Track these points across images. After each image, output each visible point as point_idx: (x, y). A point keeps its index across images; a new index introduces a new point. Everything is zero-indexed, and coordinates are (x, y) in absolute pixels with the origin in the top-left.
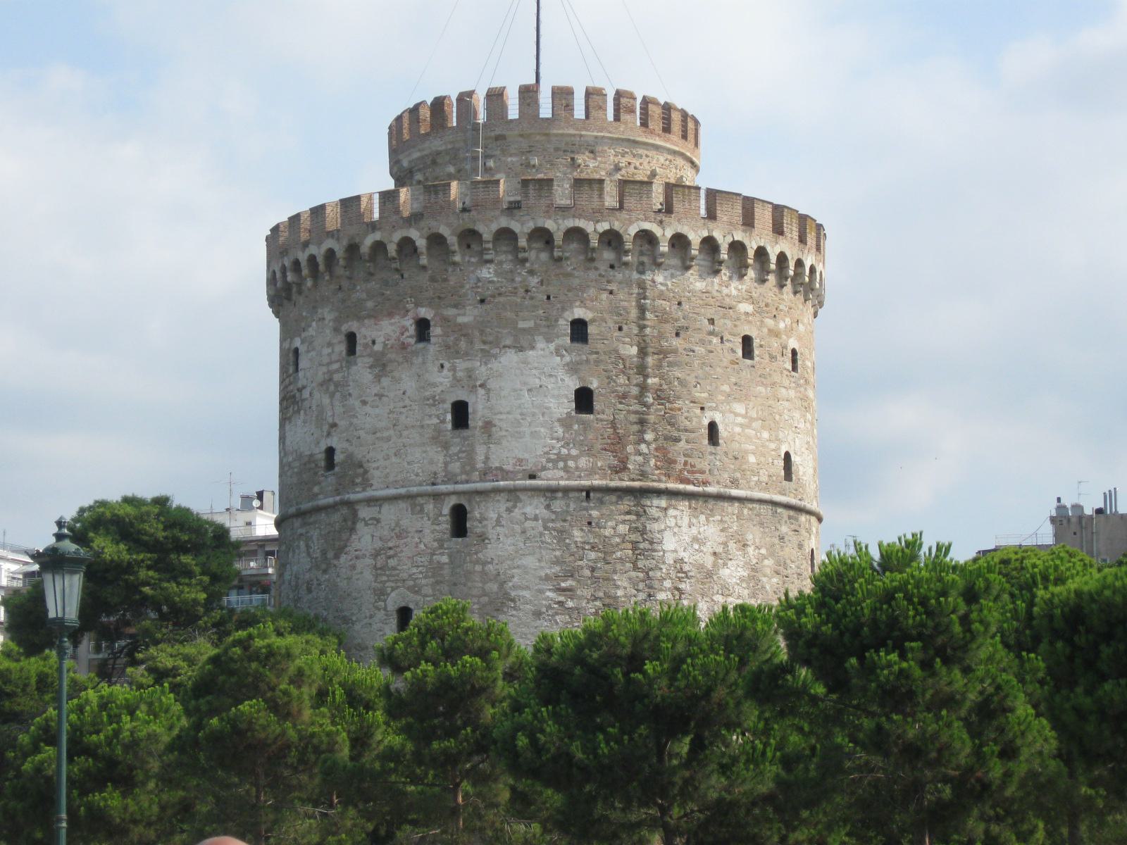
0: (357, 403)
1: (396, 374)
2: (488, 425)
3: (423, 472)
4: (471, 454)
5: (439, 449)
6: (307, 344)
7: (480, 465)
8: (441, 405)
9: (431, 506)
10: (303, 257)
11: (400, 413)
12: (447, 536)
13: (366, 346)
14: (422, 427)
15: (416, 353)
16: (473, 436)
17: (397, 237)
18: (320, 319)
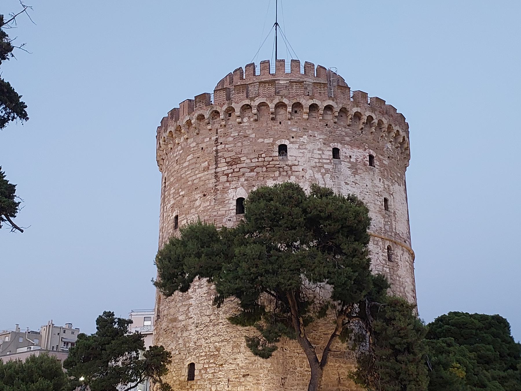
0: (343, 183)
1: (362, 175)
2: (394, 213)
3: (376, 225)
4: (391, 224)
5: (382, 217)
6: (298, 145)
7: (394, 230)
8: (381, 197)
9: (381, 243)
10: (306, 103)
11: (366, 194)
12: (387, 259)
13: (346, 157)
14: (375, 204)
15: (371, 169)
16: (391, 216)
17: (368, 114)
18: (310, 136)
